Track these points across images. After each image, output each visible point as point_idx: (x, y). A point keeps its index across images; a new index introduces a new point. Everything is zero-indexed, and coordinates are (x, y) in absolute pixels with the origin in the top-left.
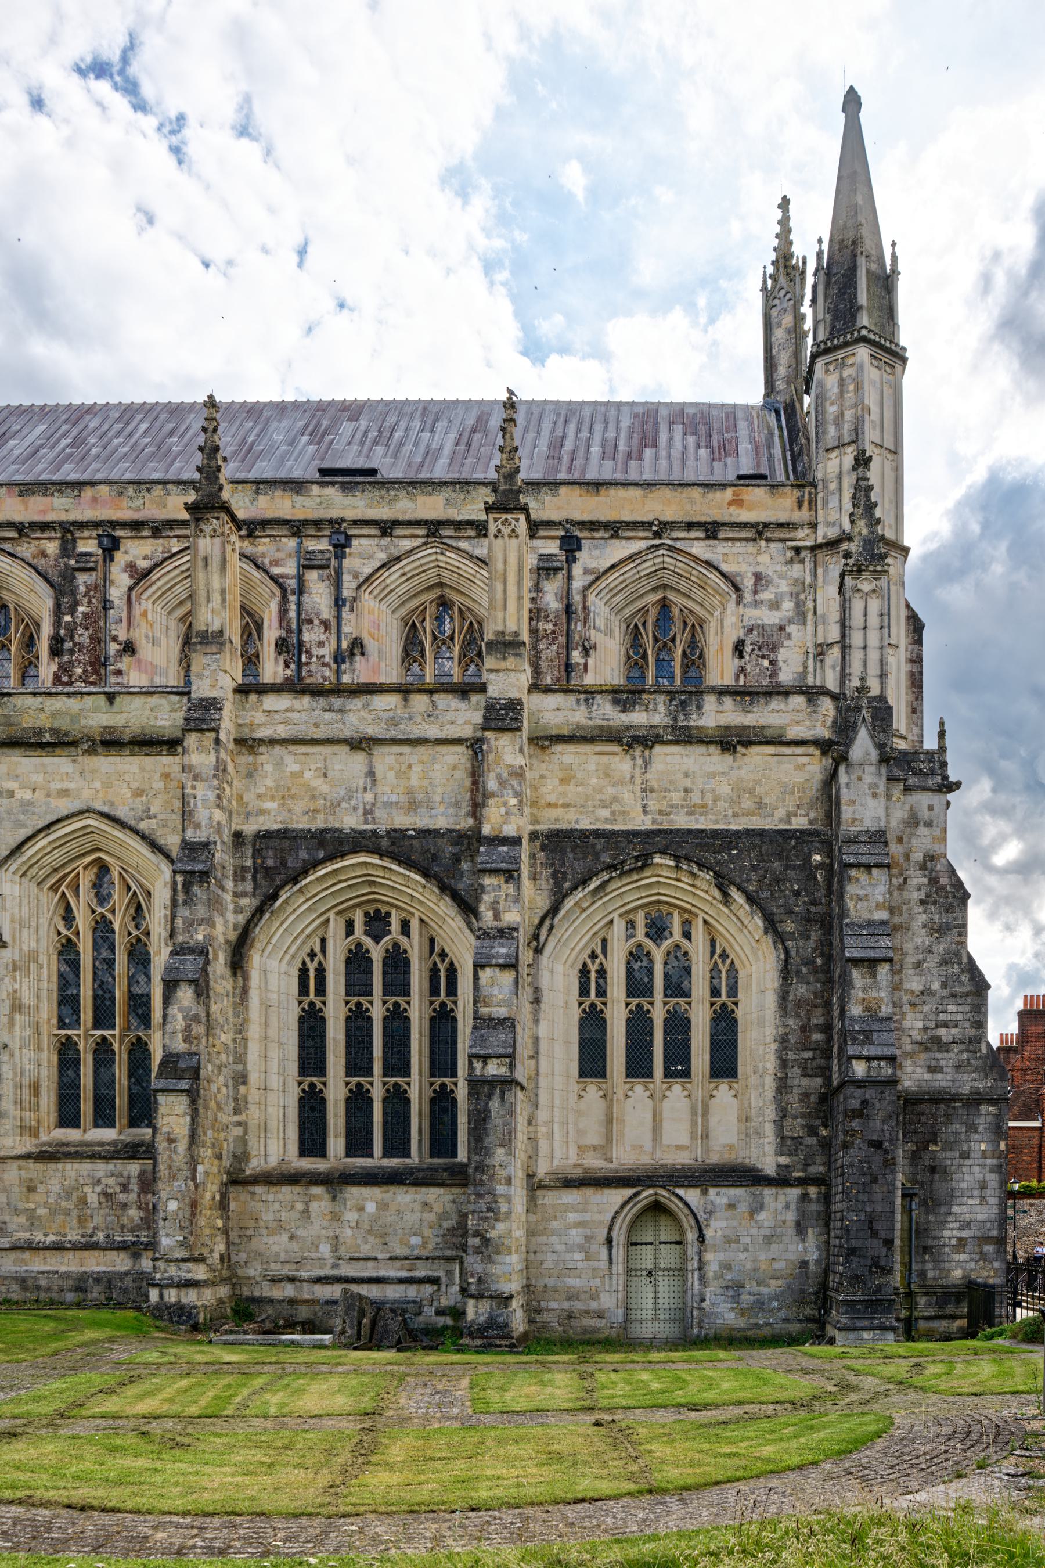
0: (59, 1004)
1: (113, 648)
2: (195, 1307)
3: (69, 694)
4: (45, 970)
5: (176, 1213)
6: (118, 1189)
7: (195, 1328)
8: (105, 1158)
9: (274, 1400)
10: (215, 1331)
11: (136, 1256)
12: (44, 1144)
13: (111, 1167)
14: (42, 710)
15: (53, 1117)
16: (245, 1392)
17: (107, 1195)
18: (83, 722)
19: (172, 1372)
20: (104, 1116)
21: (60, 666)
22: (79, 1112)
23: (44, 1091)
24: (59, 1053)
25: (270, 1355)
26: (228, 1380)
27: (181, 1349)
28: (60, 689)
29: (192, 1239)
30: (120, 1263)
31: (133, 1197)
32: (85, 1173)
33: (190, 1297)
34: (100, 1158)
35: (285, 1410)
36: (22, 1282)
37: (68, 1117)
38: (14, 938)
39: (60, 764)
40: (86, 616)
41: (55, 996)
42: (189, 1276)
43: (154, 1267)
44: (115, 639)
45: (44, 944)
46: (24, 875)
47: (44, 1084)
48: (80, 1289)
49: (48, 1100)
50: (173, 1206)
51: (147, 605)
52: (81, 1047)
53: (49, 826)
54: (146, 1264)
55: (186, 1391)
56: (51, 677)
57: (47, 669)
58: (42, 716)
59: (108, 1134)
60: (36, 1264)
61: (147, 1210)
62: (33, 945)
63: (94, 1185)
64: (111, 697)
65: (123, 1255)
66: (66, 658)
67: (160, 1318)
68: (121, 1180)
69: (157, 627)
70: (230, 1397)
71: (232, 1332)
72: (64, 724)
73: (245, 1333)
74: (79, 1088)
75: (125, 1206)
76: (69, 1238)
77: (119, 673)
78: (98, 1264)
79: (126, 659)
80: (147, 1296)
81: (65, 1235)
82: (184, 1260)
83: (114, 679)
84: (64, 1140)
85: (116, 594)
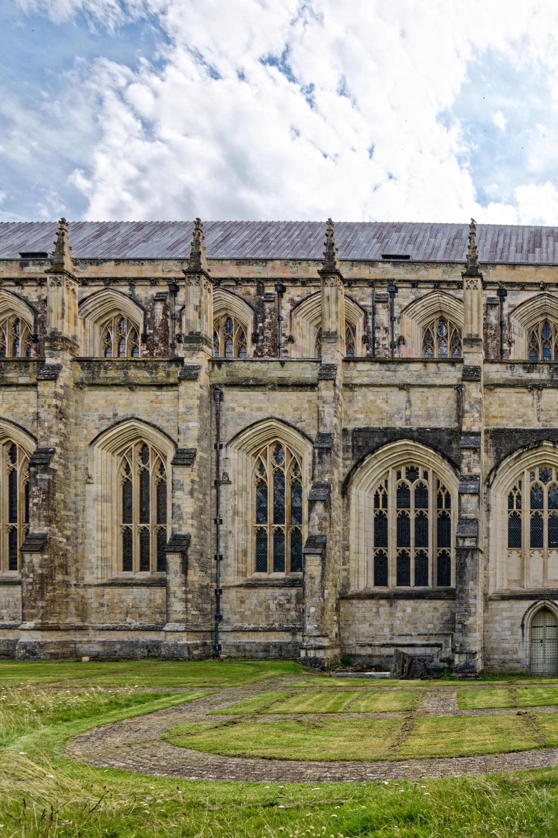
0: (257, 512)
1: (283, 339)
2: (323, 659)
3: (262, 361)
4: (250, 495)
5: (314, 613)
6: (285, 602)
7: (323, 669)
8: (279, 586)
9: (363, 704)
10: (333, 671)
11: (294, 634)
12: (249, 580)
13: (282, 591)
14: (249, 369)
15: (254, 566)
16: (349, 700)
17: (280, 605)
18: (269, 375)
19: (312, 692)
20: (279, 566)
21: (257, 348)
22: (266, 564)
23: (249, 555)
24: (257, 536)
25: (360, 682)
26: (340, 695)
27: (316, 680)
28: (257, 359)
29: (322, 626)
30: (286, 638)
31: (293, 605)
32: (269, 594)
33: (321, 654)
34: (277, 586)
35: (368, 709)
36: (238, 647)
37: (261, 566)
38: (235, 479)
39: (257, 395)
40: (270, 324)
41: (255, 507)
42: (320, 644)
43: (303, 640)
44: (284, 335)
45: (250, 482)
46: (240, 449)
47: (249, 550)
48: (265, 651)
49: (251, 558)
50: (313, 610)
51: (299, 319)
52: (268, 532)
53: (252, 425)
54: (299, 638)
55: (319, 700)
56: (252, 353)
57: (251, 349)
58: (249, 372)
59: (281, 575)
60: (244, 639)
61: (300, 612)
62: (244, 483)
63: (274, 600)
64: (282, 363)
65: (287, 634)
66: (260, 344)
67: (306, 665)
68: (287, 597)
69: (304, 329)
70: (341, 703)
71: (341, 671)
72: (259, 376)
73: (347, 671)
74: (266, 553)
75: (289, 610)
76: (261, 626)
77: (286, 351)
78: (275, 639)
79: (290, 345)
80: (299, 654)
81: (259, 624)
82: (318, 636)
83: (283, 354)
84: (259, 578)
85: (284, 313)
